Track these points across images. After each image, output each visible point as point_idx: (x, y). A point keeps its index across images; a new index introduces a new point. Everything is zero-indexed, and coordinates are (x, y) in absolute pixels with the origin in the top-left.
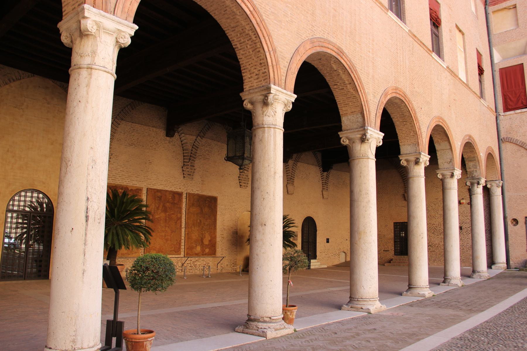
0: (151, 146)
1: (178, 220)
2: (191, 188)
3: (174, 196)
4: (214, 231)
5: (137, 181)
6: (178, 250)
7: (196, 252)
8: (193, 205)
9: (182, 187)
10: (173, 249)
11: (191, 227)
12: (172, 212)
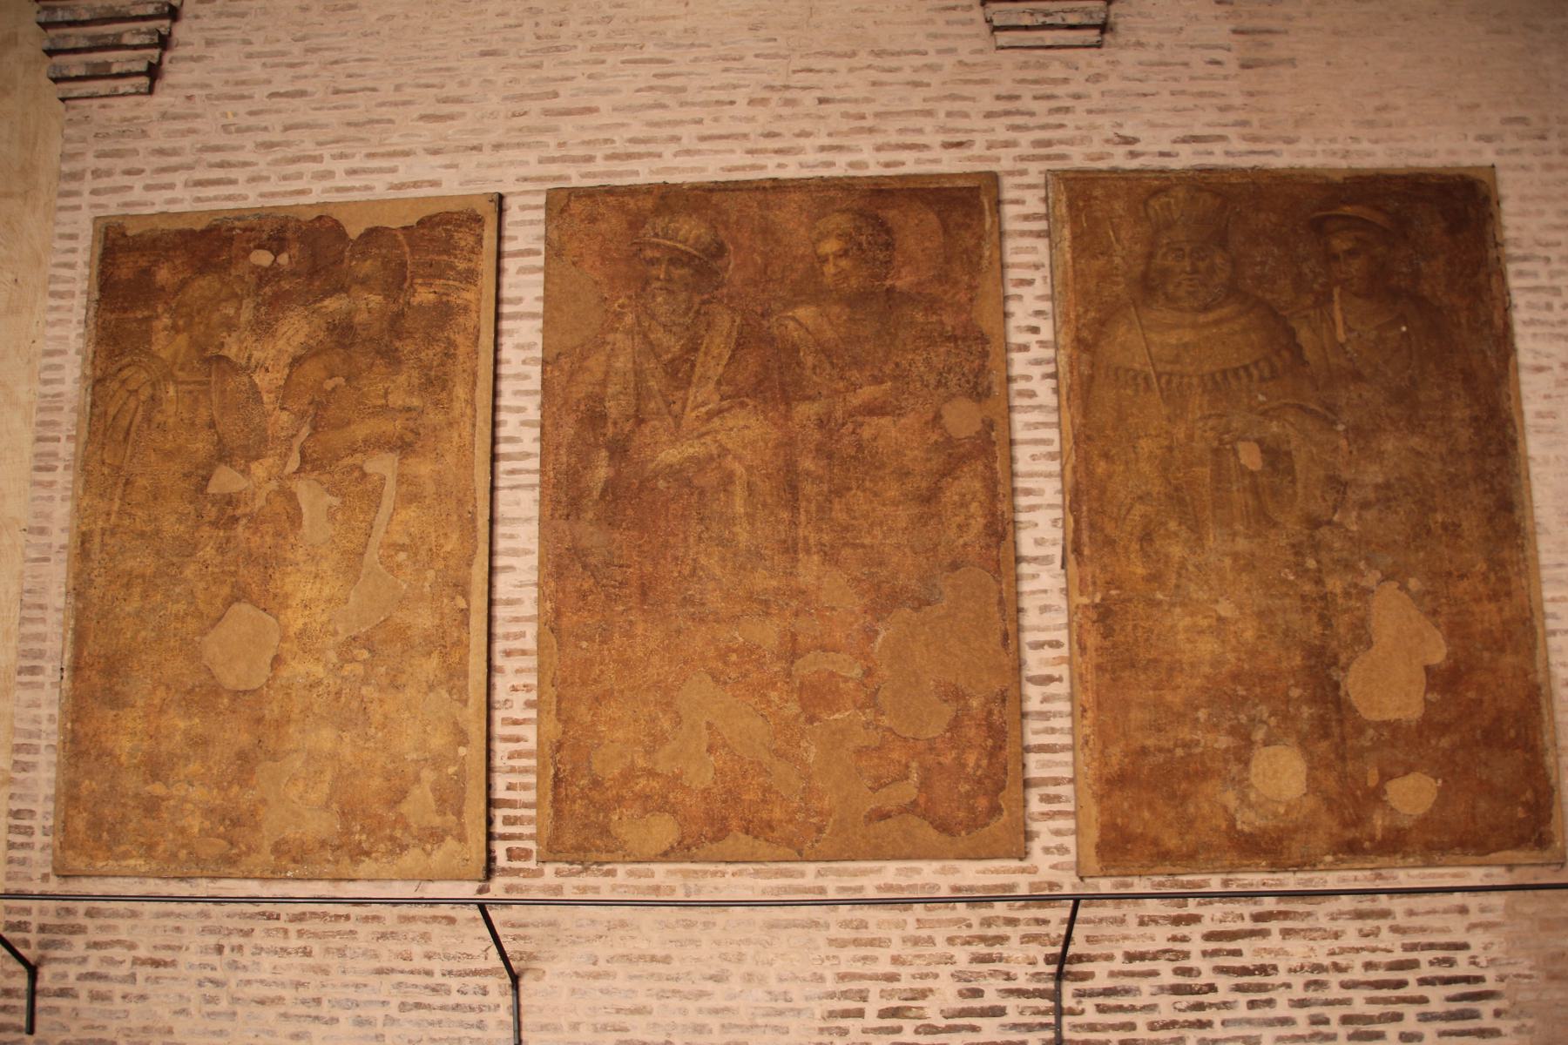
1: (949, 471)
2: (1105, 121)
3: (883, 226)
4: (1496, 564)
5: (436, 152)
6: (982, 803)
7: (1248, 821)
8: (1149, 286)
9: (978, 123)
10: (909, 790)
11: (1147, 537)
12: (868, 393)
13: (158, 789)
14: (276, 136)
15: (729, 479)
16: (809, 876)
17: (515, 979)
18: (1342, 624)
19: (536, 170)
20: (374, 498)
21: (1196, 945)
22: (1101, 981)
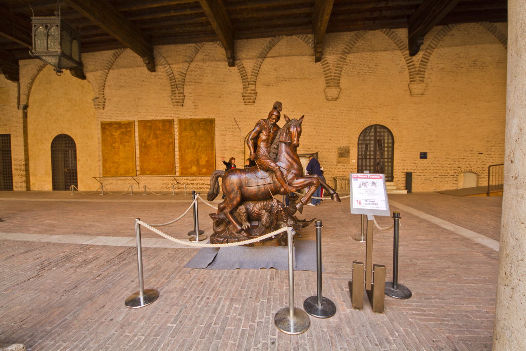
0: (138, 85)
1: (170, 145)
2: (183, 114)
3: (164, 124)
4: (211, 152)
8: (185, 129)
10: (166, 169)
11: (185, 150)
12: (163, 138)
13: (110, 170)
14: (115, 114)
15: (153, 145)
16: (160, 176)
17: (139, 184)
18: (199, 157)
19: (137, 118)
20: (126, 146)
21: (188, 181)
22: (181, 184)
